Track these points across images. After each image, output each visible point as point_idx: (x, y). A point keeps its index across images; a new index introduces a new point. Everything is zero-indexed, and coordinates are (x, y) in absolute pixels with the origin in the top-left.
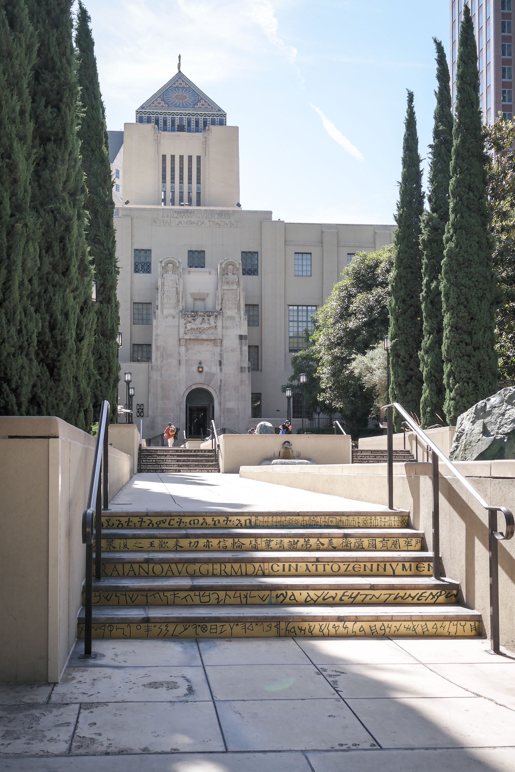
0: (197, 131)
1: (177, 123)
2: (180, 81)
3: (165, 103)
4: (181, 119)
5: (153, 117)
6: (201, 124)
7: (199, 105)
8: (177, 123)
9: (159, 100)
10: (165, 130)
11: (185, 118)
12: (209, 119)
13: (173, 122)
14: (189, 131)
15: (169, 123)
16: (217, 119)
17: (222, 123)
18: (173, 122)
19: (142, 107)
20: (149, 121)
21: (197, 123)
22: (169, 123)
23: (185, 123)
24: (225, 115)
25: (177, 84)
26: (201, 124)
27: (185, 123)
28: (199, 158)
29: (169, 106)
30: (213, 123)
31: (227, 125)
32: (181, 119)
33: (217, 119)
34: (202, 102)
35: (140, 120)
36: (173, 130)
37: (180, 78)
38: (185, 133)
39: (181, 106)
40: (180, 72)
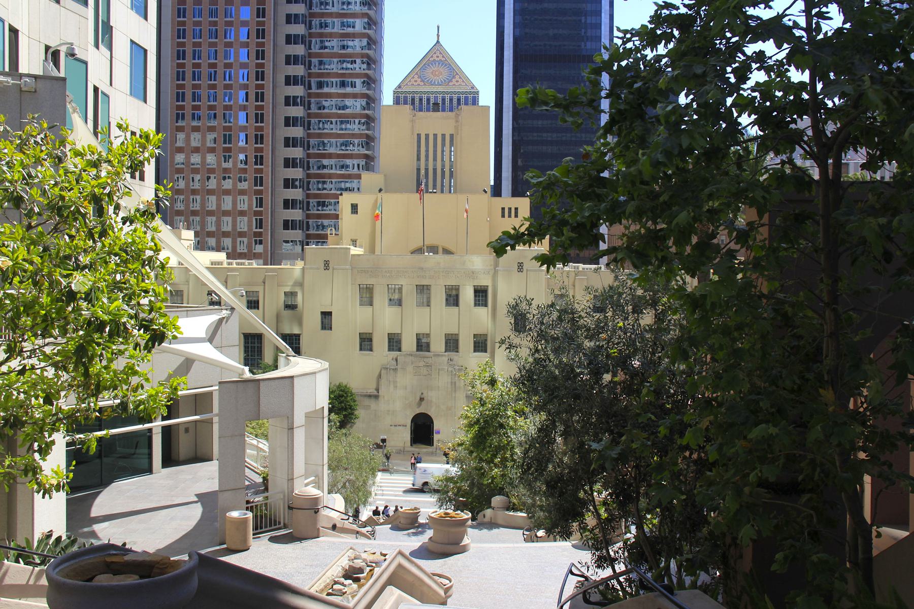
0: (451, 110)
2: (438, 54)
4: (436, 98)
5: (409, 96)
6: (455, 101)
9: (416, 77)
10: (421, 110)
11: (440, 97)
12: (462, 97)
13: (428, 100)
14: (444, 110)
15: (425, 102)
17: (475, 101)
18: (428, 100)
19: (399, 87)
20: (405, 103)
22: (425, 102)
24: (477, 93)
26: (455, 101)
28: (452, 136)
31: (480, 104)
32: (436, 98)
34: (457, 77)
35: (397, 101)
36: (428, 110)
40: (438, 42)
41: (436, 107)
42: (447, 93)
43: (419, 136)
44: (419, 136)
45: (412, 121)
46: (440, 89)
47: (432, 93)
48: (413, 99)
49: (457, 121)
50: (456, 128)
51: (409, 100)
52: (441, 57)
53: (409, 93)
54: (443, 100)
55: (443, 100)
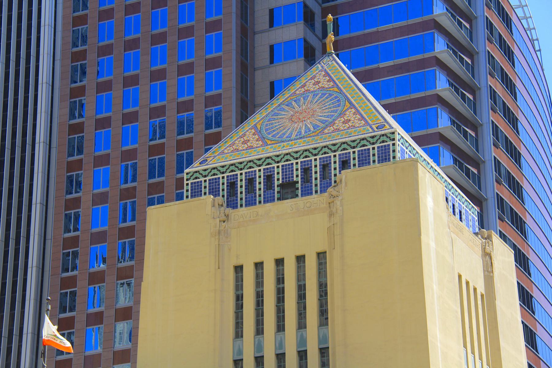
3: (262, 138)
4: (287, 170)
7: (339, 123)
12: (353, 154)
13: (269, 178)
16: (374, 150)
18: (269, 178)
27: (297, 176)
28: (321, 256)
32: (287, 170)
33: (374, 150)
38: (300, 202)
42: (315, 151)
43: (239, 269)
44: (239, 269)
45: (220, 234)
46: (300, 145)
47: (277, 159)
48: (232, 185)
49: (331, 215)
50: (330, 231)
51: (223, 187)
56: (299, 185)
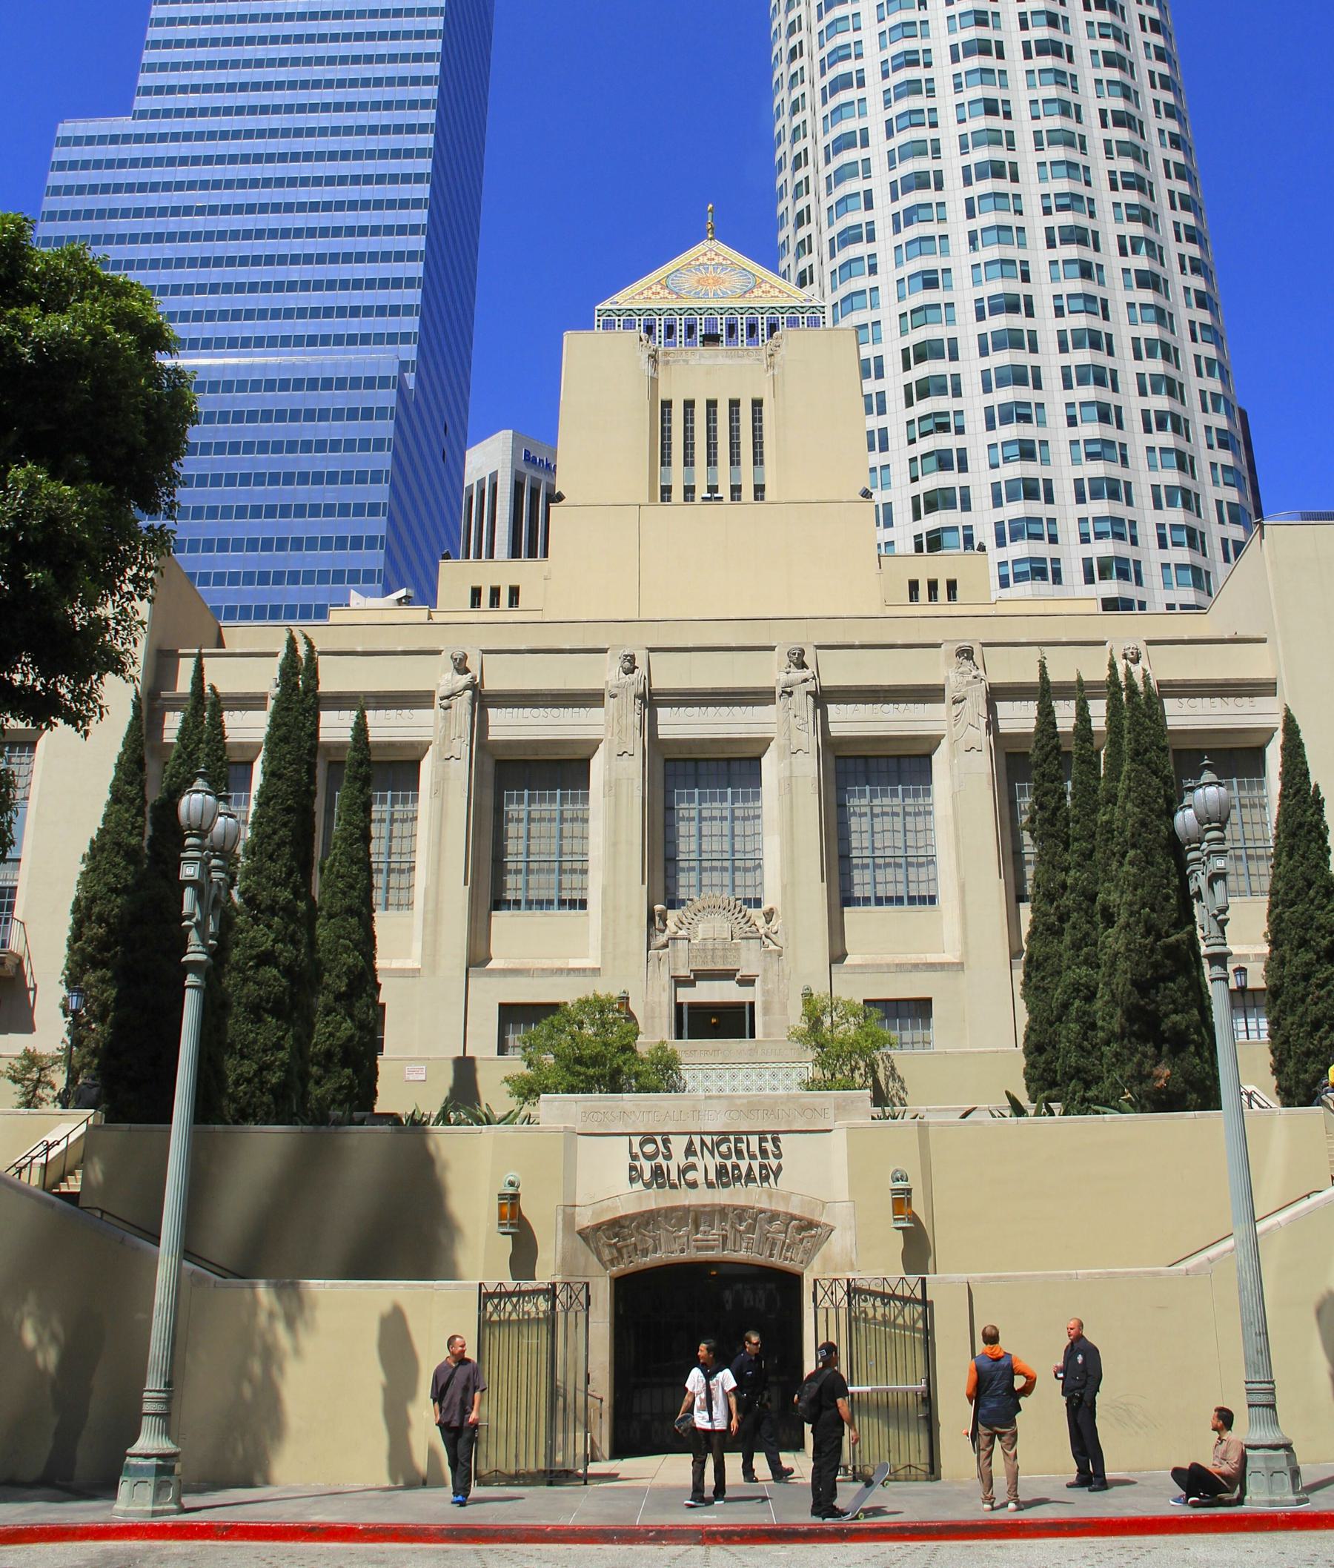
1: (700, 330)
4: (711, 323)
6: (762, 328)
7: (757, 292)
8: (700, 330)
15: (680, 330)
18: (690, 330)
20: (629, 325)
21: (752, 329)
22: (680, 330)
23: (722, 330)
25: (702, 260)
26: (762, 328)
27: (722, 330)
28: (757, 404)
29: (679, 297)
30: (793, 323)
32: (711, 323)
34: (765, 287)
37: (711, 250)
39: (711, 295)
41: (711, 339)
43: (667, 405)
52: (719, 260)
53: (640, 312)
54: (732, 329)
55: (732, 329)
56: (724, 339)
